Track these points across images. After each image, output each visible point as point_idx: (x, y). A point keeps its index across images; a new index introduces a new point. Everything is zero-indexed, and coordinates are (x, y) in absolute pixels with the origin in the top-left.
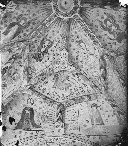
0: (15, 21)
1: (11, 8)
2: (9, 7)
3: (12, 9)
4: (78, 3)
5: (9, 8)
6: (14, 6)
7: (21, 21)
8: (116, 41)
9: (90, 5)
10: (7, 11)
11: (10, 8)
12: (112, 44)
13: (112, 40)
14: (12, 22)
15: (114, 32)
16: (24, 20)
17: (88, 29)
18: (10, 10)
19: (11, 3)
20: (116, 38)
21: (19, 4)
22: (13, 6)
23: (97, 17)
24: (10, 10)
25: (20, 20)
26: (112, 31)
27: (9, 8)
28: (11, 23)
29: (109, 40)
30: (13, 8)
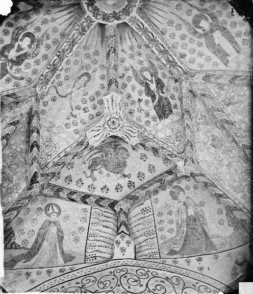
4: (86, 3)
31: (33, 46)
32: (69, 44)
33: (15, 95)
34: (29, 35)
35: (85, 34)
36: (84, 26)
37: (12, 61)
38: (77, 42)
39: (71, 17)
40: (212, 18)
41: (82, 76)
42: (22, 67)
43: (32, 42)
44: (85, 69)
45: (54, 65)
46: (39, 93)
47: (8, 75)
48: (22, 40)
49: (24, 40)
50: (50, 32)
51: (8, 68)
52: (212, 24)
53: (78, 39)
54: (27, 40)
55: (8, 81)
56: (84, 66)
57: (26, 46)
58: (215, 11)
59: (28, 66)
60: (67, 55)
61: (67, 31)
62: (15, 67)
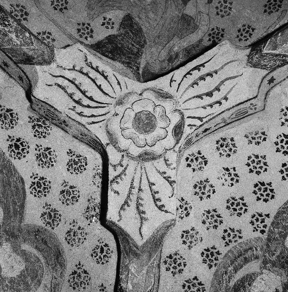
0: (33, 212)
1: (133, 205)
2: (140, 190)
3: (126, 203)
5: (136, 184)
6: (142, 218)
7: (25, 255)
10: (120, 169)
11: (136, 190)
14: (28, 191)
16: (22, 275)
18: (117, 193)
19: (161, 208)
21: (145, 257)
22: (141, 213)
24: (117, 193)
25: (26, 247)
27: (132, 187)
28: (27, 186)
30: (131, 211)
40: (246, 261)
52: (265, 262)
58: (224, 250)
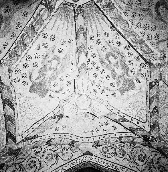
8: (30, 83)
9: (81, 25)
12: (22, 80)
13: (30, 78)
15: (44, 75)
17: (37, 30)
20: (37, 81)
23: (59, 42)
26: (44, 73)
29: (28, 74)
31: (116, 55)
32: (119, 24)
33: (152, 82)
34: (107, 56)
35: (114, 4)
36: (104, 4)
37: (125, 73)
38: (119, 14)
39: (97, 18)
41: (157, 11)
42: (131, 67)
43: (113, 55)
44: (151, 8)
45: (136, 42)
46: (159, 62)
47: (134, 80)
48: (110, 62)
49: (111, 61)
50: (107, 39)
51: (129, 78)
53: (116, 12)
54: (111, 58)
55: (138, 81)
56: (148, 8)
57: (115, 60)
59: (131, 63)
60: (130, 27)
61: (109, 24)
62: (129, 73)
